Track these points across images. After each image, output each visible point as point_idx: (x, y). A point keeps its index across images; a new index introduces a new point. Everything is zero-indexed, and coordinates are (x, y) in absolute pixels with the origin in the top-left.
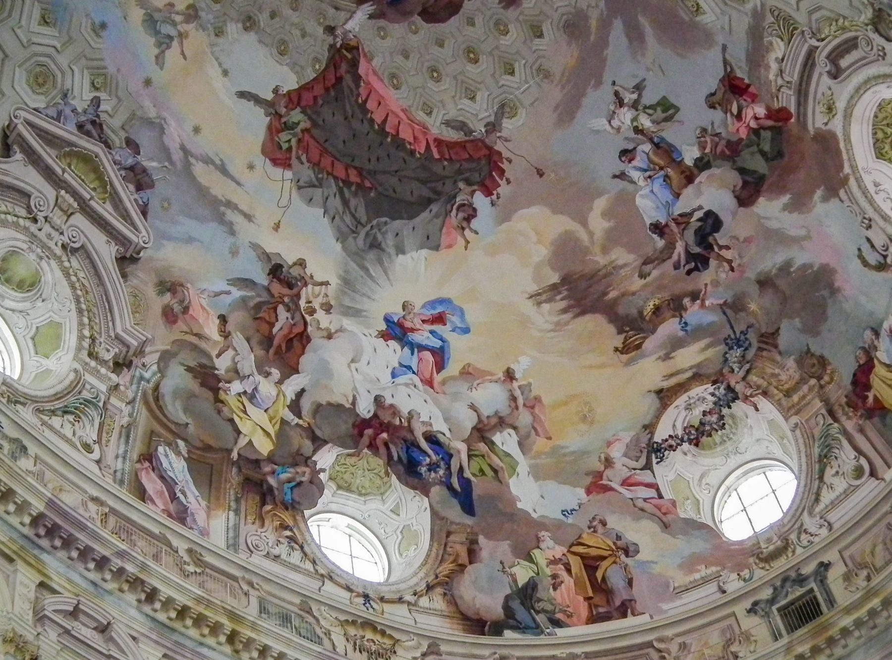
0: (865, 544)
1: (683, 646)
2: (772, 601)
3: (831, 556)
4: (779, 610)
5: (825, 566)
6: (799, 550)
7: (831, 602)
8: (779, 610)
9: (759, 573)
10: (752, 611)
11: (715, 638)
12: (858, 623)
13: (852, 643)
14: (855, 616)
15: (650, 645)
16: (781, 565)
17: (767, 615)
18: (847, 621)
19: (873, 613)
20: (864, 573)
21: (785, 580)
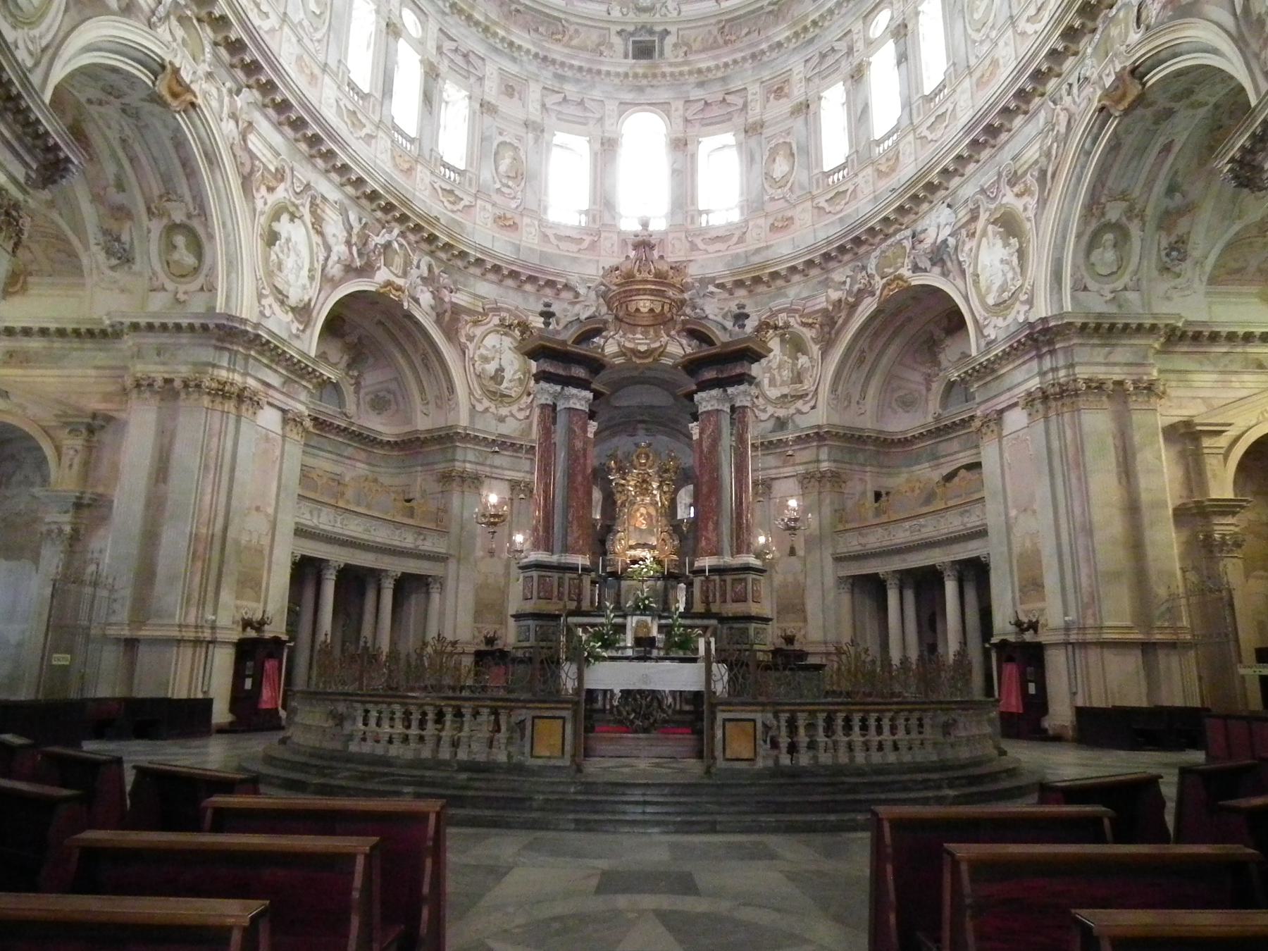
0: (693, 33)
1: (577, 31)
2: (632, 34)
3: (673, 29)
4: (634, 42)
5: (667, 32)
6: (658, 15)
7: (661, 53)
8: (634, 42)
9: (631, 15)
10: (619, 33)
11: (594, 37)
12: (672, 74)
13: (663, 82)
14: (672, 69)
15: (560, 20)
16: (645, 18)
17: (626, 40)
18: (668, 70)
19: (681, 74)
20: (685, 49)
21: (643, 27)
